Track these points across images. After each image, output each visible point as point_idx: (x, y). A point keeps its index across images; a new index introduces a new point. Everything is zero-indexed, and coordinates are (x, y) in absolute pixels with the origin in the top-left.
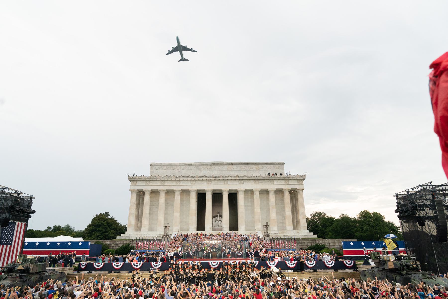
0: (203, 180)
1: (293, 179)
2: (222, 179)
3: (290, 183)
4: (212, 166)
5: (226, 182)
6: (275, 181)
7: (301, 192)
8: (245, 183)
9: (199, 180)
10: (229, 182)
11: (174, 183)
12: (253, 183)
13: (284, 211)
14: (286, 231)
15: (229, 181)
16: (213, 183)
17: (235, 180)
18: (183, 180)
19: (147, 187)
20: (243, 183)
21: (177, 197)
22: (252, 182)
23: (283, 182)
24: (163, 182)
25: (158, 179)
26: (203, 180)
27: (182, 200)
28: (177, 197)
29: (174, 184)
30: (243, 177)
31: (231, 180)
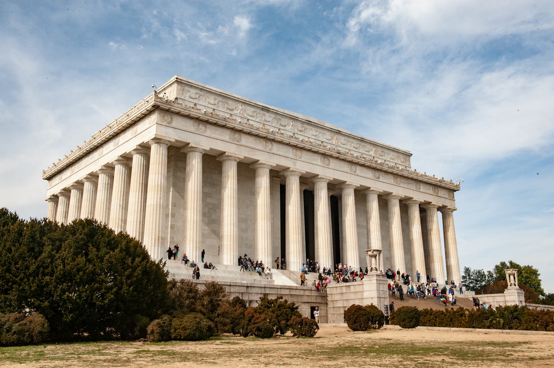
2: (349, 158)
4: (306, 126)
5: (353, 167)
8: (381, 179)
10: (359, 170)
11: (259, 145)
15: (359, 168)
16: (333, 163)
18: (281, 142)
20: (378, 178)
22: (390, 179)
23: (430, 190)
24: (237, 135)
25: (230, 125)
29: (260, 147)
31: (363, 165)
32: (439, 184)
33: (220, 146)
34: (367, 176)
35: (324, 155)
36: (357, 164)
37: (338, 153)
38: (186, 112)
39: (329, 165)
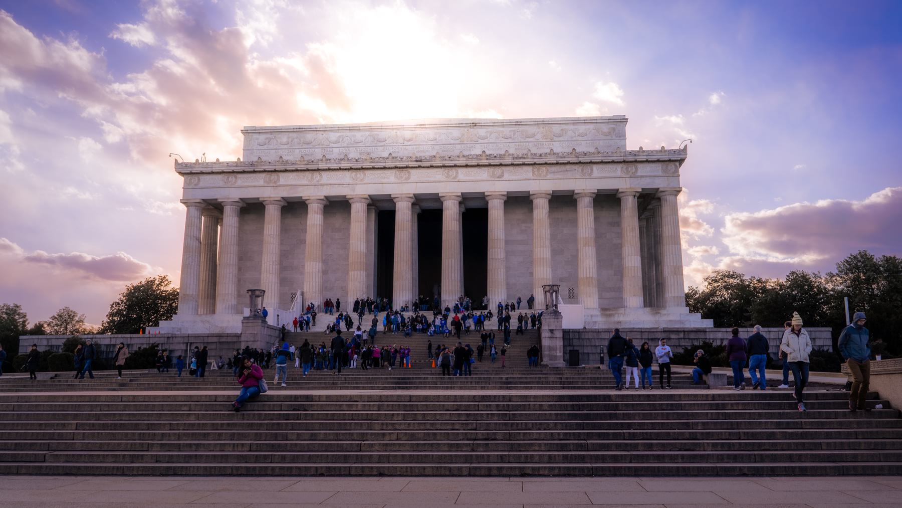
0: (385, 168)
1: (647, 161)
2: (439, 163)
3: (639, 173)
6: (595, 167)
7: (670, 198)
8: (506, 176)
9: (374, 168)
12: (530, 175)
13: (620, 256)
14: (622, 311)
15: (460, 170)
17: (478, 166)
18: (329, 169)
19: (233, 192)
20: (502, 176)
21: (315, 218)
23: (618, 170)
24: (274, 176)
26: (385, 168)
27: (326, 227)
28: (315, 218)
30: (501, 157)
31: (467, 166)
32: (631, 158)
33: (251, 194)
34: (479, 178)
35: (396, 168)
36: (455, 166)
37: (417, 161)
38: (209, 170)
39: (409, 178)
